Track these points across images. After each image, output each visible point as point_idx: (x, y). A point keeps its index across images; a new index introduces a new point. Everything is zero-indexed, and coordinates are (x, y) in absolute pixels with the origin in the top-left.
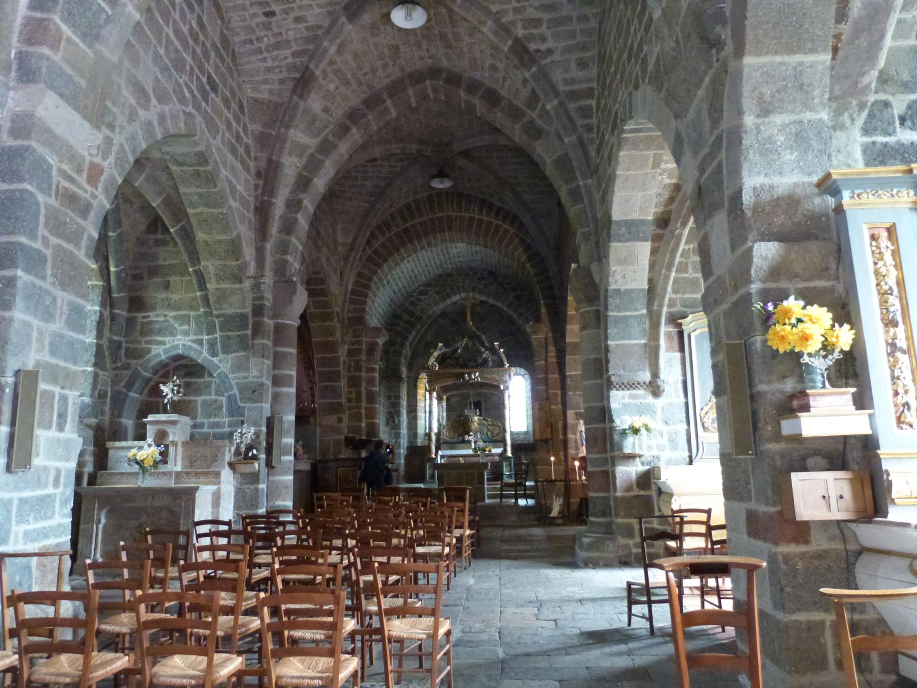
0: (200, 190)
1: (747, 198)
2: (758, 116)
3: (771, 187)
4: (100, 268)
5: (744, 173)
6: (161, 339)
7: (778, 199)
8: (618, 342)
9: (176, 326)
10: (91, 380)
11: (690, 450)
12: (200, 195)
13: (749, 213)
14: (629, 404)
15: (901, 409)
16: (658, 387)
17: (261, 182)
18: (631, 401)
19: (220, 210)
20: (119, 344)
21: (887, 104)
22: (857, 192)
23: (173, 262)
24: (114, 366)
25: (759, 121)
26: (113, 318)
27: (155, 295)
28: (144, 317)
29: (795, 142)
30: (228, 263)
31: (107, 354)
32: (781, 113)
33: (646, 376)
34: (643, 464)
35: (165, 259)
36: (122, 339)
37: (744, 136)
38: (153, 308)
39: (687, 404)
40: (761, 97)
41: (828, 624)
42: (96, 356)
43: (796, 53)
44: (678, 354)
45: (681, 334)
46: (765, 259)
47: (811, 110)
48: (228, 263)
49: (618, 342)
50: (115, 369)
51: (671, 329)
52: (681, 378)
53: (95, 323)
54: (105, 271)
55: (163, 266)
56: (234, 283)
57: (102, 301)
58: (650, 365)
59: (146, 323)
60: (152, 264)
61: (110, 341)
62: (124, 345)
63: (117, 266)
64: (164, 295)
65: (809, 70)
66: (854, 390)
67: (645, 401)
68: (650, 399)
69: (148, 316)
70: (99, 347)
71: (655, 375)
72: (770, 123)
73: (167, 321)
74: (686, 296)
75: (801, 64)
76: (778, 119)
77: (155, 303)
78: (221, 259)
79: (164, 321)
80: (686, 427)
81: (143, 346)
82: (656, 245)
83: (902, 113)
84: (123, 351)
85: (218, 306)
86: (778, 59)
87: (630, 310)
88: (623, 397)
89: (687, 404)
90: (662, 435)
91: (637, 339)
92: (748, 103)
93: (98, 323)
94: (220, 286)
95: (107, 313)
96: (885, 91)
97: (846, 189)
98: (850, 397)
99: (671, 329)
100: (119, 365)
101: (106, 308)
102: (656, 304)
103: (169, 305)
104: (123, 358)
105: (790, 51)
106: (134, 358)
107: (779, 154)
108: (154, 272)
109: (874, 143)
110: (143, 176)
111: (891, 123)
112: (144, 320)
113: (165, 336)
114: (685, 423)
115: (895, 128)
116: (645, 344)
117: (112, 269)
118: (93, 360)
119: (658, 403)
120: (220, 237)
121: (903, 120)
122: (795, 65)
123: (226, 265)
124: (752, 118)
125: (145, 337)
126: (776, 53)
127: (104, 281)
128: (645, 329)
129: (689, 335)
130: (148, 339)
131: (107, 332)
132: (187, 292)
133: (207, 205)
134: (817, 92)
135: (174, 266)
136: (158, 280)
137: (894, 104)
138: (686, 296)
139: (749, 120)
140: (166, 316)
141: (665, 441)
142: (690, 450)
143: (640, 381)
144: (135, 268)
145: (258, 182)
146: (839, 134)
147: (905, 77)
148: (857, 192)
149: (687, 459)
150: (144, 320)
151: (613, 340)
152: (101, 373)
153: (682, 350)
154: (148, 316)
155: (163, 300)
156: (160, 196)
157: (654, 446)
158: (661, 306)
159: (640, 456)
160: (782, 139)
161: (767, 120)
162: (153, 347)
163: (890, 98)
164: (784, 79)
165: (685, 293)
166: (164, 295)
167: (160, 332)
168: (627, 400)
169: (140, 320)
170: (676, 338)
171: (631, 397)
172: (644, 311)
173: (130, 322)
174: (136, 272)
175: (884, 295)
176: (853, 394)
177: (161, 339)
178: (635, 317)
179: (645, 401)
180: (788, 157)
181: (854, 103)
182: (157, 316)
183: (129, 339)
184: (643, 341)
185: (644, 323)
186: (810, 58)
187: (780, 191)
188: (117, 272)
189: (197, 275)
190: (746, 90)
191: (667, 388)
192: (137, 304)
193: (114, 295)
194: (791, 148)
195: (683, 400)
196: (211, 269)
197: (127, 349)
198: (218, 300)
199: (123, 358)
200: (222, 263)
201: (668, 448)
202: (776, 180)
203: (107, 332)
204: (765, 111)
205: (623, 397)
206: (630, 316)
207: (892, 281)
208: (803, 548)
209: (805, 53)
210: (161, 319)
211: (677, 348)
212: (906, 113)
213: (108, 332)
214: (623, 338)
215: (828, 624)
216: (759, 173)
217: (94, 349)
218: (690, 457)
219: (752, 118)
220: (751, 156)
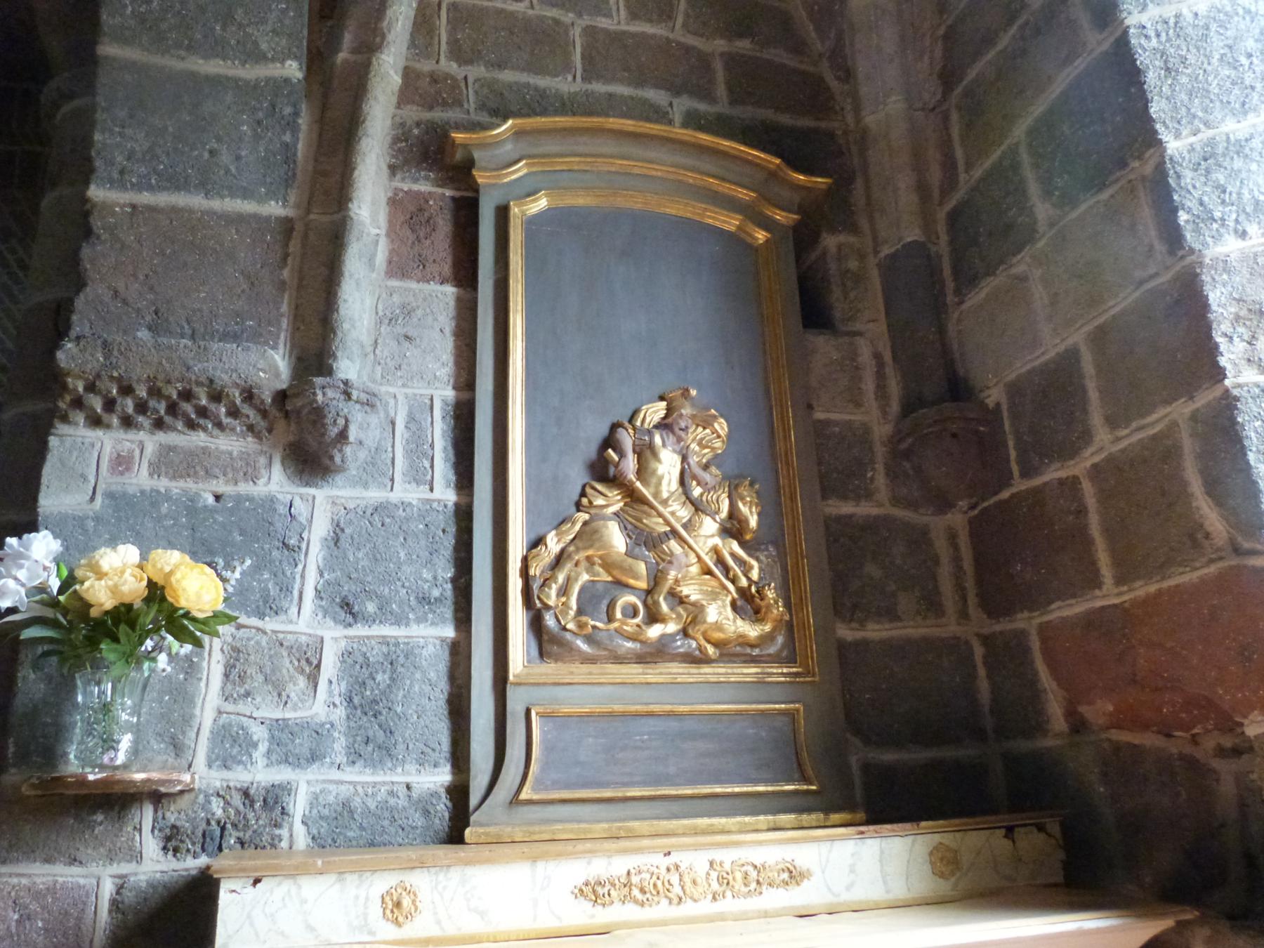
8: (146, 198)
11: (460, 757)
14: (154, 498)
16: (318, 414)
18: (163, 484)
33: (273, 365)
34: (172, 841)
39: (464, 516)
44: (450, 290)
45: (465, 212)
49: (146, 198)
51: (424, 187)
58: (298, 317)
67: (244, 488)
68: (275, 482)
71: (314, 358)
74: (508, 76)
80: (449, 632)
87: (217, 49)
88: (122, 463)
89: (464, 516)
90: (313, 679)
91: (246, 194)
99: (424, 187)
102: (348, 39)
114: (448, 612)
116: (287, 227)
119: (318, 507)
128: (288, 149)
129: (503, 214)
138: (508, 76)
141: (323, 706)
142: (460, 757)
143: (224, 379)
149: (443, 807)
151: (120, 183)
153: (465, 275)
157: (259, 733)
159: (157, 797)
165: (500, 66)
168: (141, 479)
170: (444, 226)
171: (164, 463)
172: (293, 70)
178: (238, 85)
179: (244, 488)
184: (275, 209)
185: (292, 126)
191: (363, 429)
195: (447, 495)
201: (340, 744)
205: (122, 463)
206: (217, 82)
211: (447, 269)
214: (176, 183)
218: (458, 793)
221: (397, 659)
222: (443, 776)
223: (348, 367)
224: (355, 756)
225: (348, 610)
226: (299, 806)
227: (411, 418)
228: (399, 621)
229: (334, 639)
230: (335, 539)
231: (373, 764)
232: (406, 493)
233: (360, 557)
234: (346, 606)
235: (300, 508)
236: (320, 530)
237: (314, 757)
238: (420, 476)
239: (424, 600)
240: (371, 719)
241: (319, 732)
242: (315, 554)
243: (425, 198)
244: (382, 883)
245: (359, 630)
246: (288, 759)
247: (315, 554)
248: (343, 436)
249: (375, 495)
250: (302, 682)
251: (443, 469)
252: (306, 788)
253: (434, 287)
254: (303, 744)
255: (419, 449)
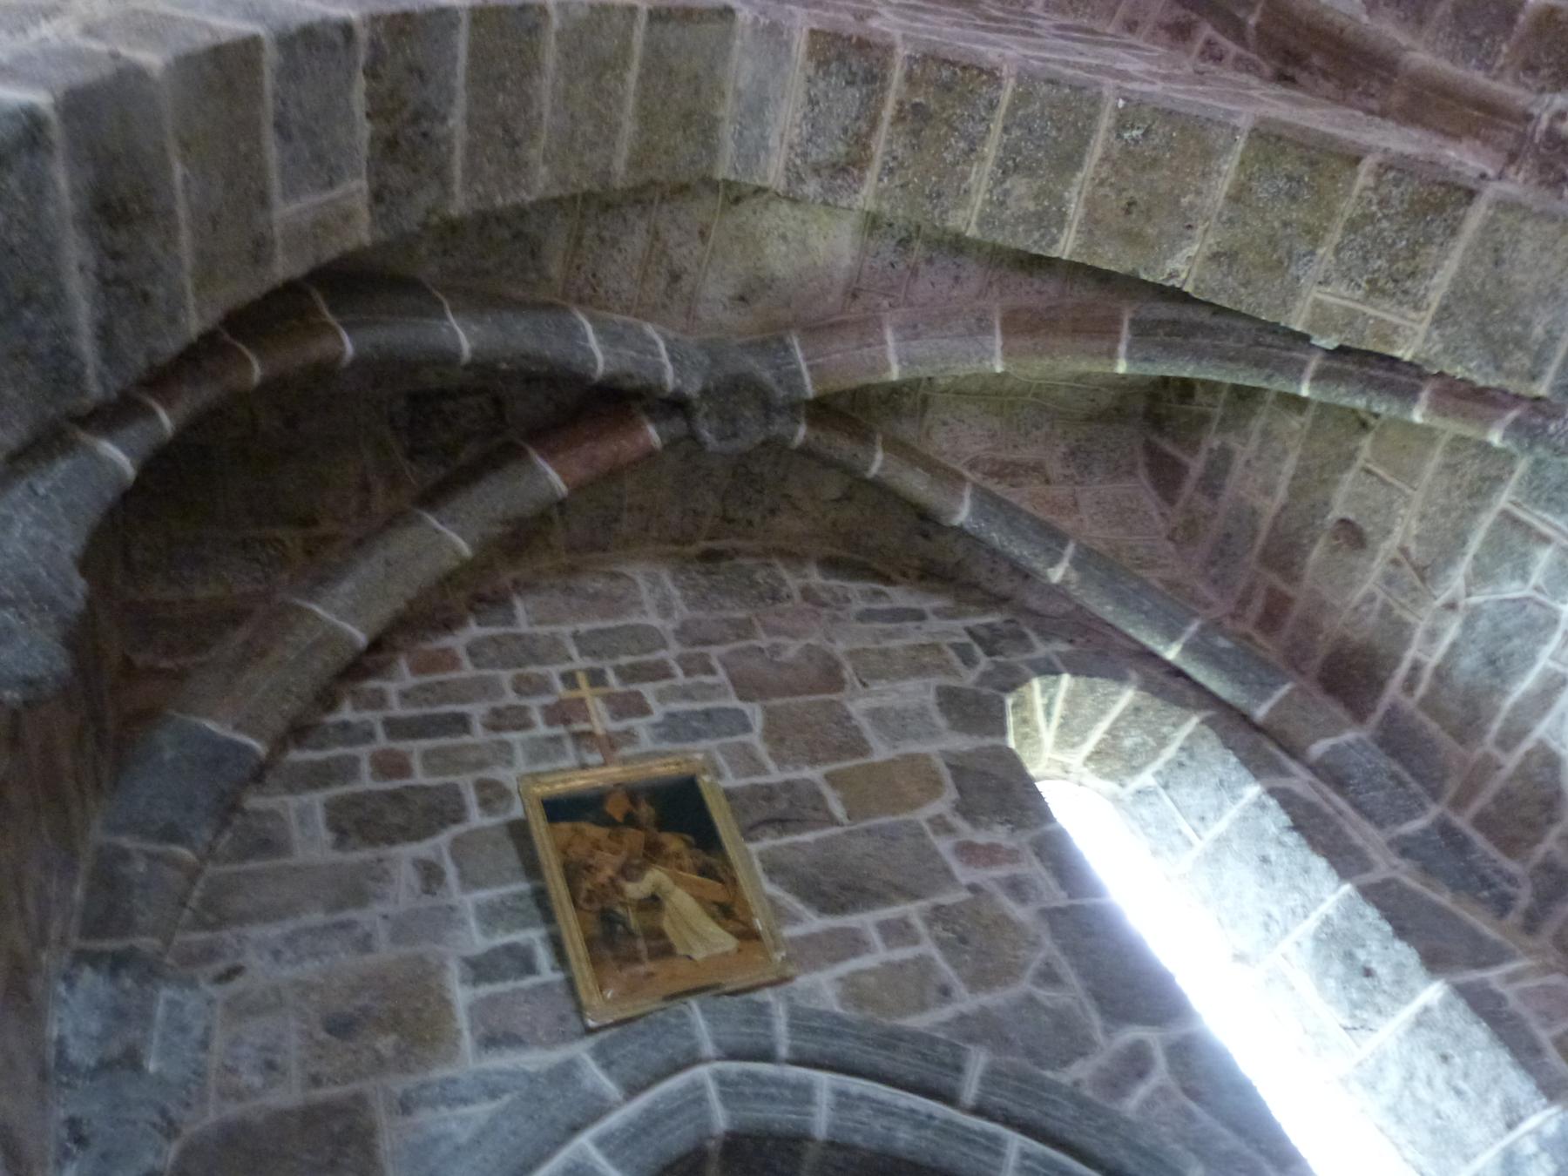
0: (991, 150)
4: (1147, 686)
6: (1526, 684)
9: (1513, 590)
10: (1480, 1033)
12: (1009, 166)
17: (1206, 31)
19: (1105, 121)
20: (1445, 829)
23: (1289, 466)
24: (1514, 918)
26: (1332, 774)
27: (1358, 595)
28: (1410, 685)
30: (1348, 208)
31: (1444, 899)
35: (1268, 491)
36: (1434, 811)
38: (1400, 632)
42: (1401, 932)
48: (1348, 208)
50: (1531, 924)
53: (1292, 839)
54: (1177, 685)
55: (1284, 508)
56: (1454, 232)
57: (1245, 762)
59: (1433, 691)
60: (1260, 541)
61: (1404, 848)
62: (1462, 822)
63: (1172, 636)
64: (1378, 566)
69: (1416, 668)
70: (1382, 896)
73: (1474, 614)
77: (1386, 610)
78: (1314, 235)
79: (1468, 625)
81: (1511, 762)
84: (1479, 840)
85: (1521, 360)
93: (1297, 826)
94: (1435, 299)
95: (1300, 781)
100: (1525, 898)
101: (1283, 772)
103: (1420, 571)
104: (1512, 866)
106: (1535, 829)
108: (1284, 554)
110: (889, 336)
112: (1421, 690)
113: (1529, 659)
117: (1172, 653)
118: (1405, 953)
120: (1222, 187)
123: (1352, 226)
125: (1481, 732)
127: (1197, 708)
130: (1496, 726)
131: (1363, 834)
132: (1412, 477)
133: (1069, 161)
135: (1303, 471)
136: (1317, 553)
140: (1451, 606)
144: (1244, 602)
145: (1198, 45)
150: (1421, 690)
152: (1493, 976)
154: (1416, 668)
155: (1389, 580)
156: (988, 330)
162: (1541, 729)
166: (1378, 566)
167: (1500, 667)
169: (1410, 703)
173: (1398, 740)
174: (1258, 605)
177: (1526, 684)
182: (1433, 635)
183: (1452, 787)
188: (1189, 648)
189: (1340, 377)
192: (1351, 676)
193: (1261, 712)
196: (1338, 296)
197: (1481, 822)
198: (1497, 350)
199: (1512, 866)
200: (1335, 237)
203: (1363, 834)
210: (1452, 629)
213: (1369, 828)
217: (1371, 913)
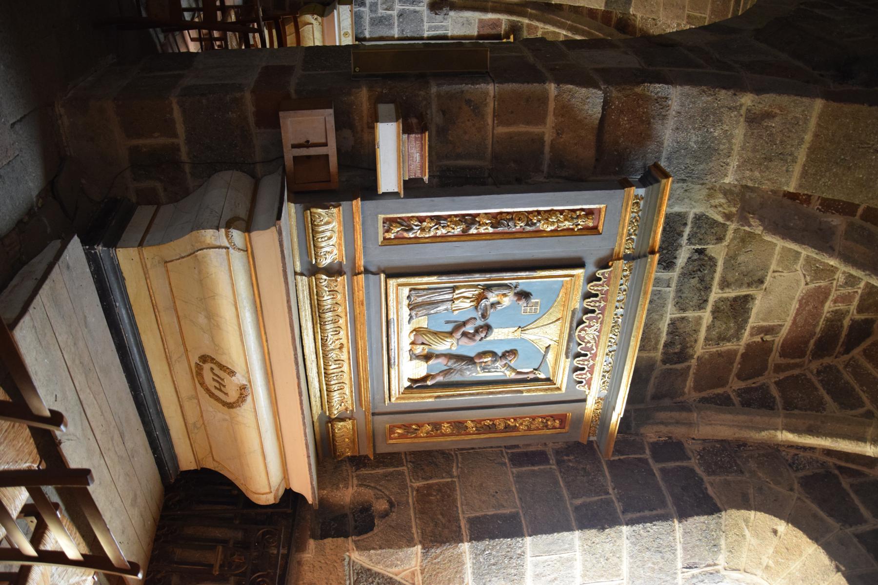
1: (658, 89)
2: (748, 111)
3: (664, 117)
5: (687, 88)
7: (649, 124)
13: (638, 90)
15: (405, 224)
16: (441, 9)
21: (720, 239)
22: (642, 203)
25: (743, 111)
29: (709, 147)
32: (745, 135)
37: (730, 93)
40: (769, 115)
41: (175, 141)
43: (808, 156)
44: (476, 34)
46: (584, 102)
47: (738, 166)
51: (503, 26)
52: (450, 34)
65: (784, 168)
66: (426, 178)
72: (738, 122)
75: (794, 161)
76: (739, 132)
80: (396, 36)
82: (599, 16)
83: (707, 252)
86: (808, 137)
90: (386, 9)
92: (769, 101)
96: (734, 239)
97: (647, 193)
98: (419, 175)
99: (503, 26)
102: (534, 11)
105: (812, 150)
107: (700, 129)
109: (685, 224)
111: (701, 241)
114: (401, 35)
115: (695, 244)
121: (701, 252)
122: (796, 154)
124: (749, 103)
126: (816, 136)
134: (757, 174)
137: (719, 246)
139: (747, 100)
141: (381, 12)
142: (371, 39)
146: (705, 192)
147: (741, 259)
148: (642, 203)
149: (362, 36)
158: (531, 17)
160: (716, 134)
161: (742, 120)
163: (725, 243)
164: (782, 142)
170: (493, 32)
175: (527, 217)
176: (422, 179)
180: (694, 138)
181: (734, 210)
186: (797, 169)
187: (657, 125)
190: (784, 100)
191: (439, 17)
194: (703, 143)
195: (426, 34)
201: (374, 16)
202: (671, 123)
204: (754, 120)
207: (541, 226)
208: (251, 120)
209: (804, 165)
211: (481, 33)
212: (706, 255)
215: (175, 141)
216: (683, 105)
219: (749, 103)
220: (705, 98)
221: (391, 26)
222: (367, 36)
223: (452, 13)
224: (371, 19)
225: (400, 15)
226: (362, 9)
227: (443, 26)
228: (398, 26)
229: (395, 13)
230: (415, 12)
231: (370, 23)
232: (426, 26)
233: (412, 17)
234: (401, 15)
235: (422, 4)
236: (417, 8)
237: (371, 11)
238: (430, 29)
239: (403, 31)
240: (378, 21)
241: (376, 11)
242: (412, 8)
243: (501, 27)
244: (350, 31)
245: (396, 18)
246: (371, 6)
247: (412, 8)
248: (436, 14)
249: (425, 19)
250: (385, 7)
251: (432, 33)
252: (365, 10)
253: (476, 30)
254: (373, 8)
255: (436, 28)
